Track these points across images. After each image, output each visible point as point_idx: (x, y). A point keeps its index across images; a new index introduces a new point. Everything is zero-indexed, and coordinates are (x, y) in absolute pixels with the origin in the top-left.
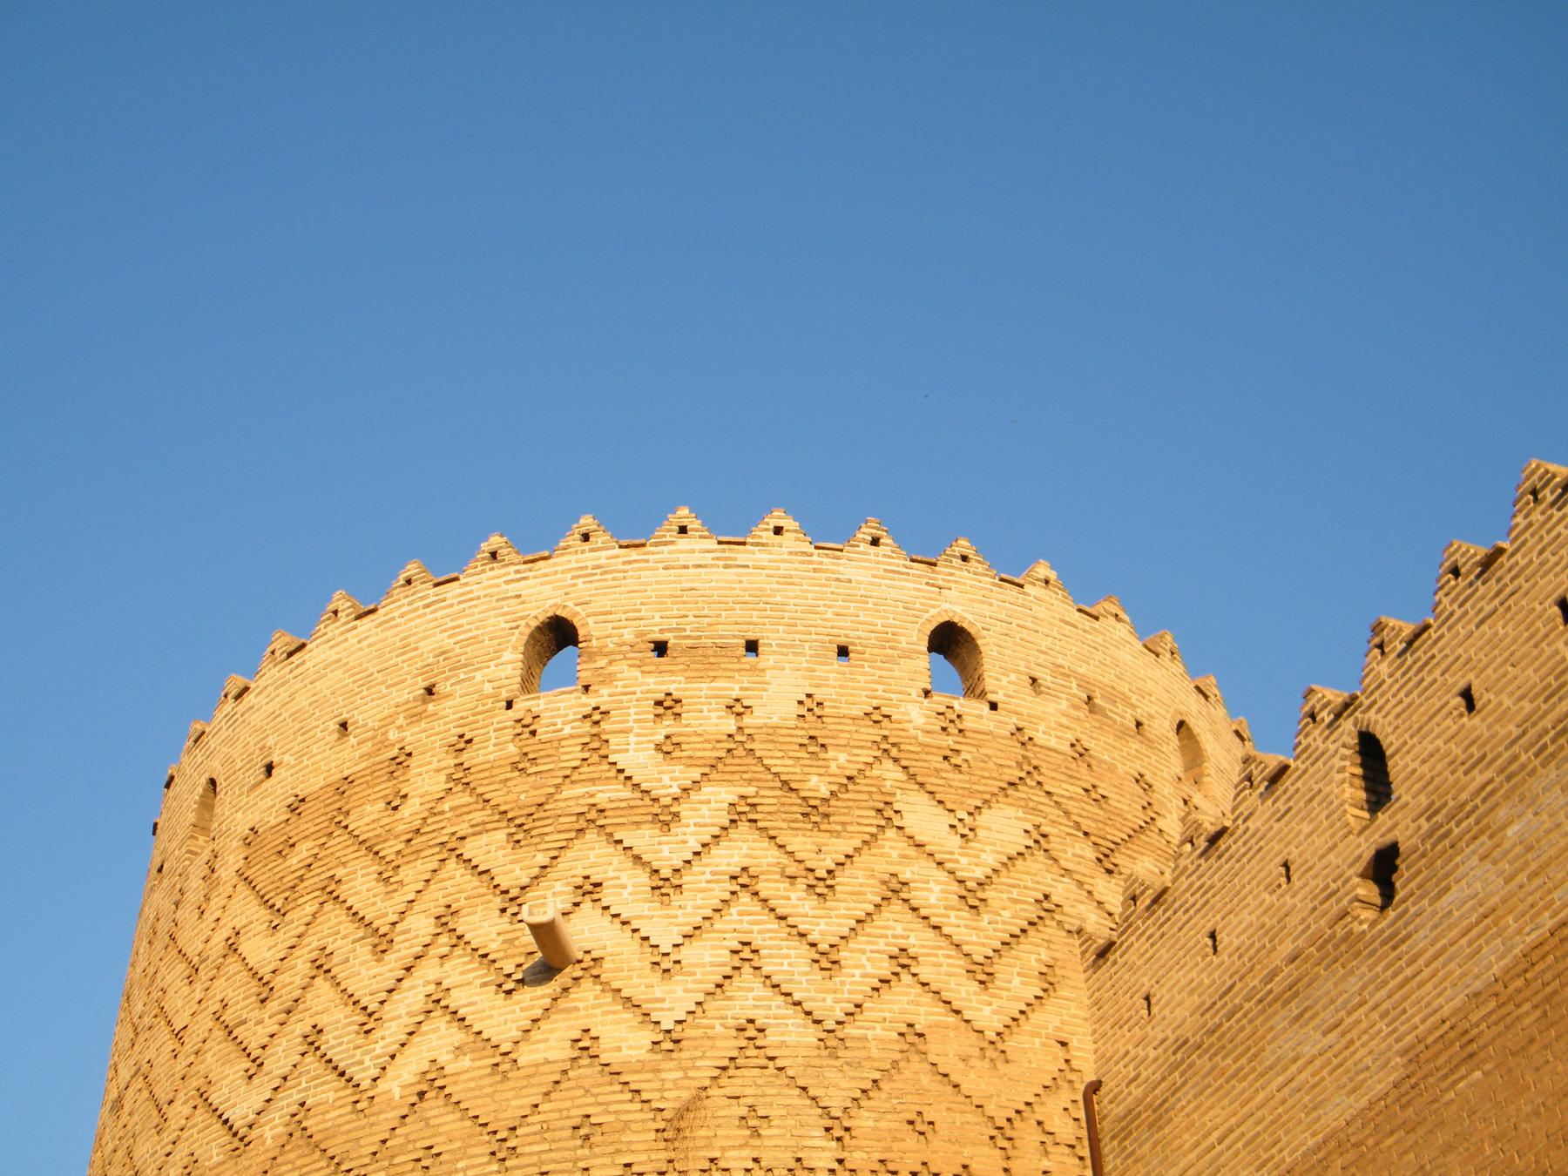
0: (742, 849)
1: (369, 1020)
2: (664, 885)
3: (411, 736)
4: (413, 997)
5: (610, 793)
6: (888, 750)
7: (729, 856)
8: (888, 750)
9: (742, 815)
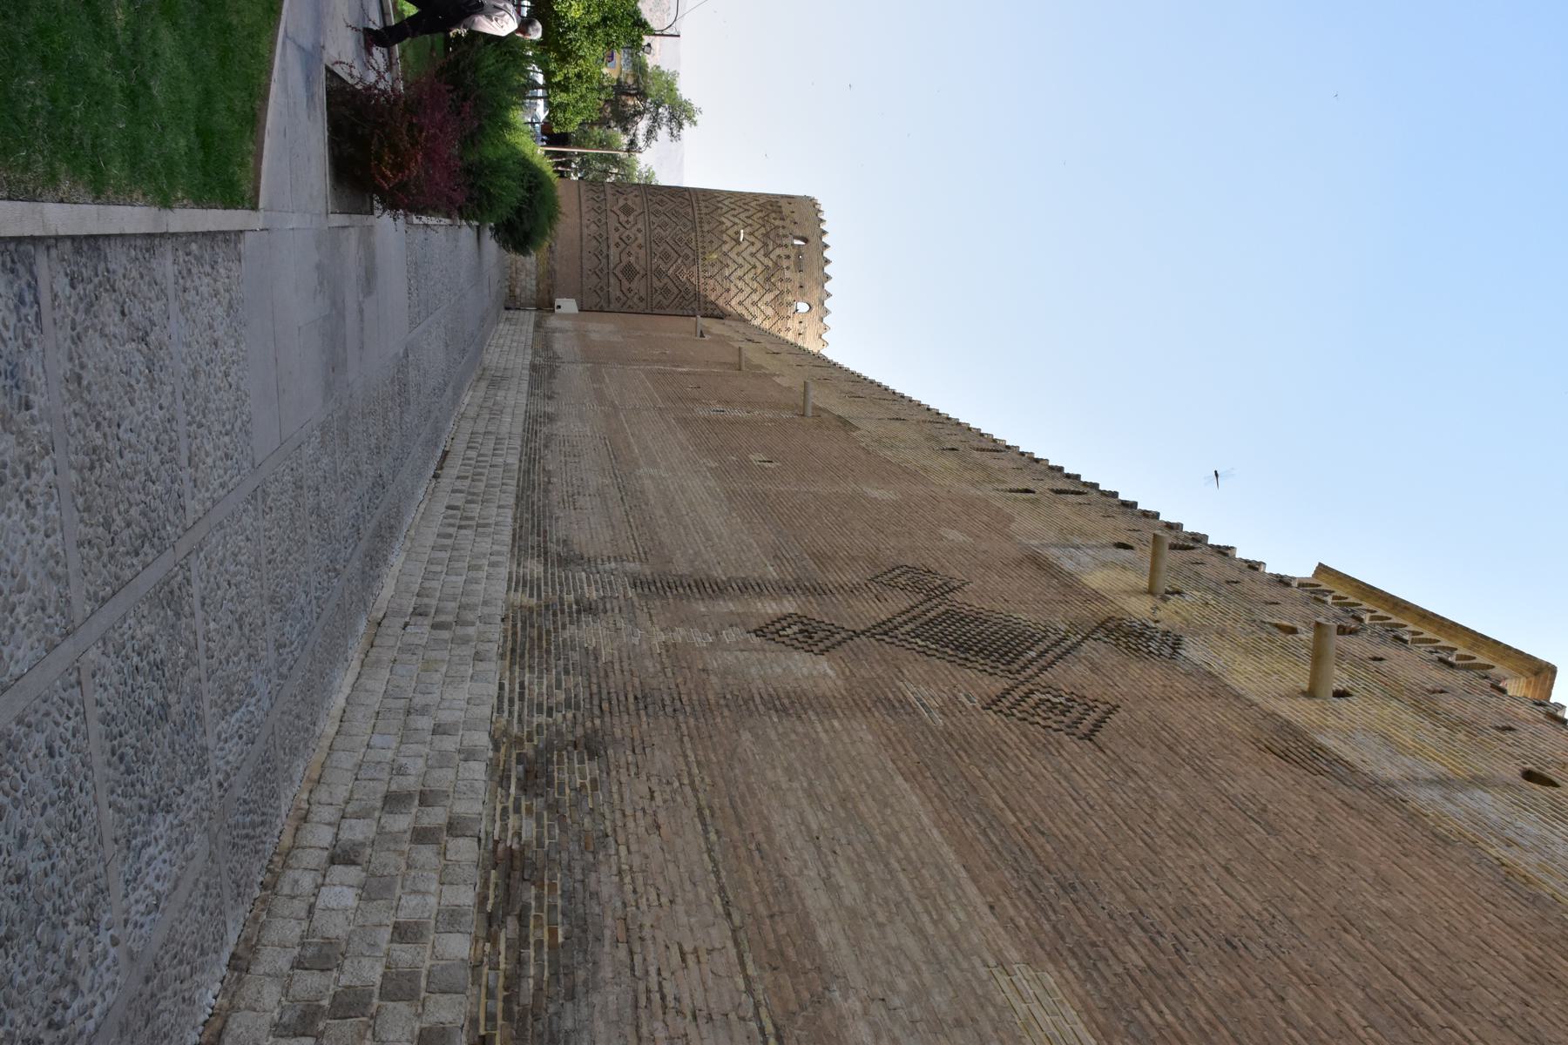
0: (760, 268)
1: (734, 216)
2: (753, 255)
3: (788, 221)
4: (737, 220)
5: (771, 248)
6: (782, 293)
7: (758, 264)
8: (782, 293)
9: (767, 267)
